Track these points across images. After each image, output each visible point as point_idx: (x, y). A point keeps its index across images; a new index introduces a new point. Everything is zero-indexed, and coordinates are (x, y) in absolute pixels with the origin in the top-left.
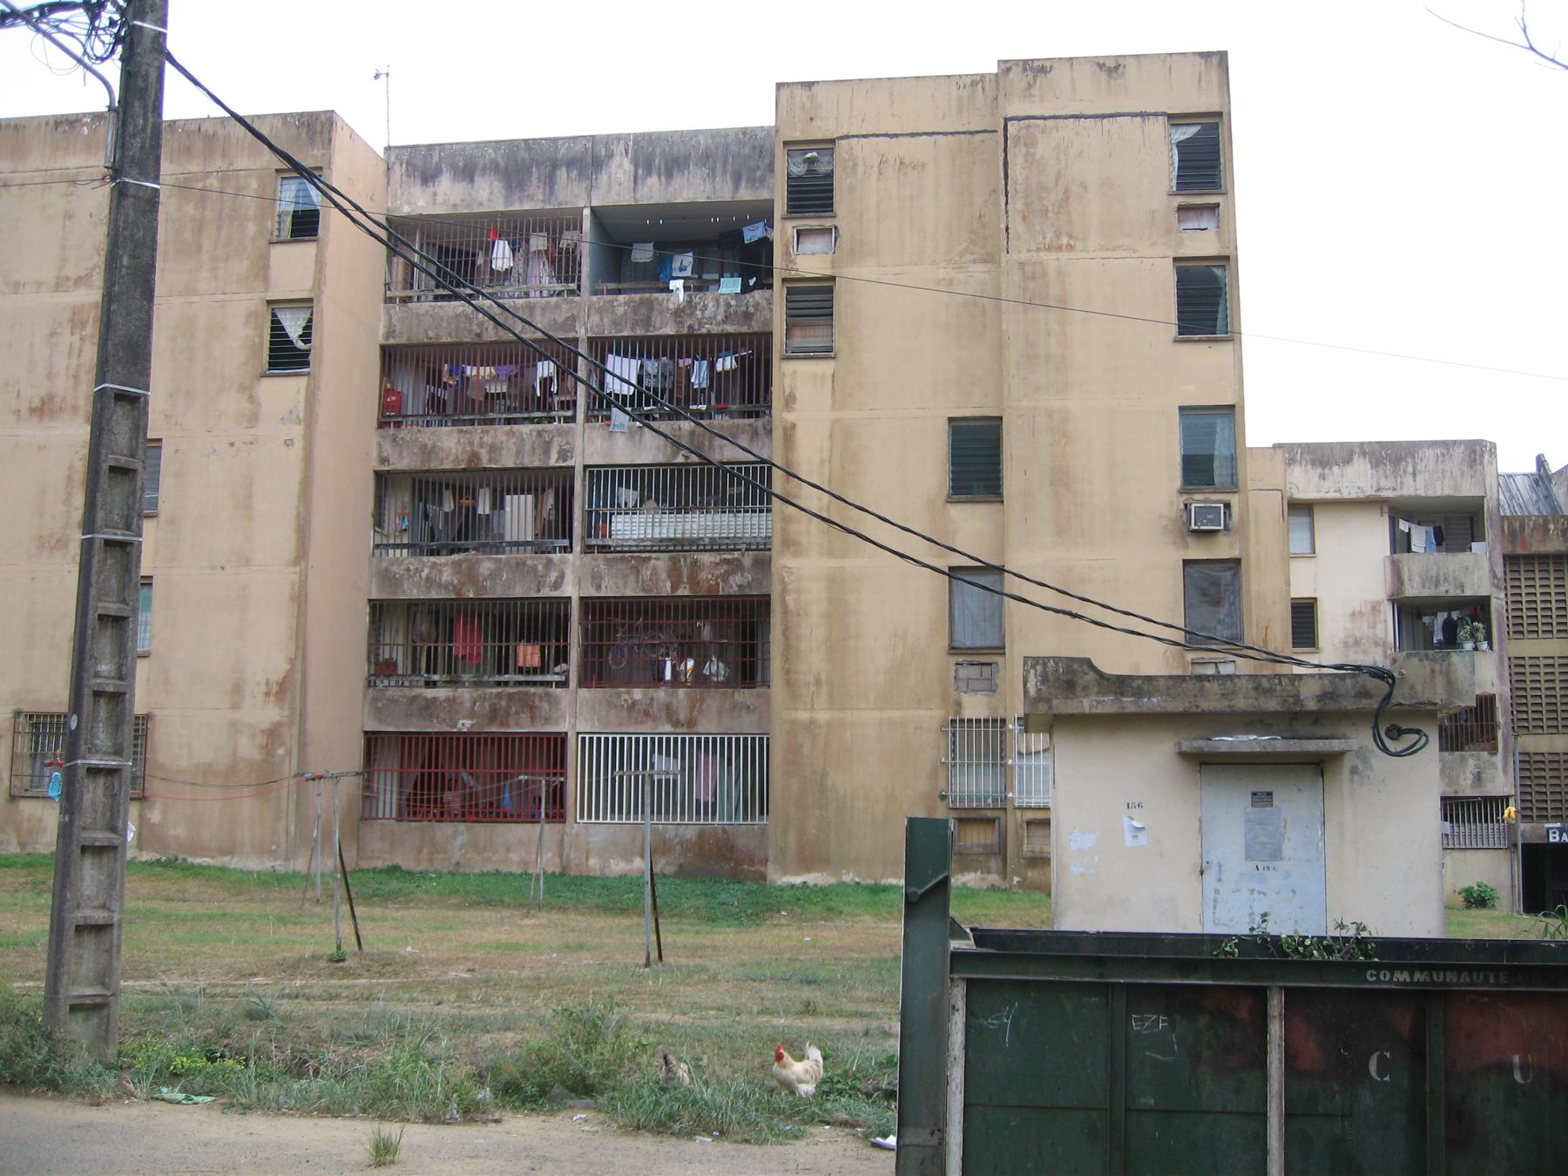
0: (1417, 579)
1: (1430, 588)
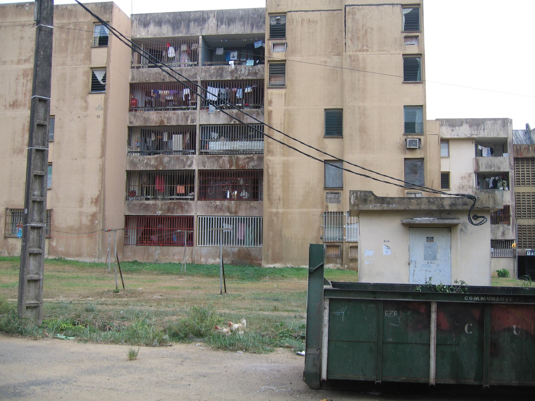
0: (484, 166)
1: (488, 169)
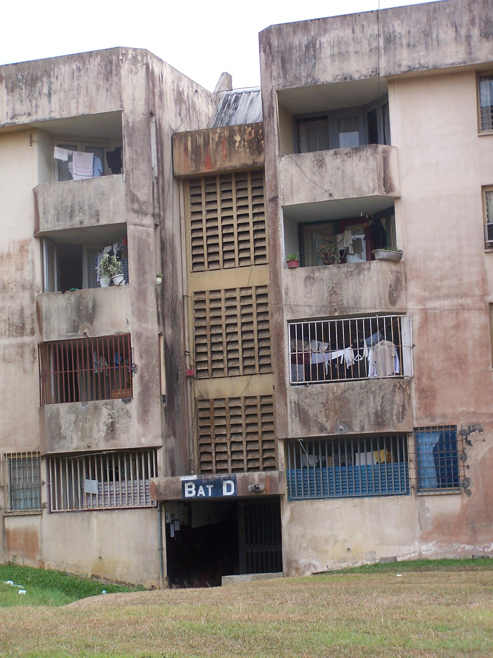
0: (52, 212)
